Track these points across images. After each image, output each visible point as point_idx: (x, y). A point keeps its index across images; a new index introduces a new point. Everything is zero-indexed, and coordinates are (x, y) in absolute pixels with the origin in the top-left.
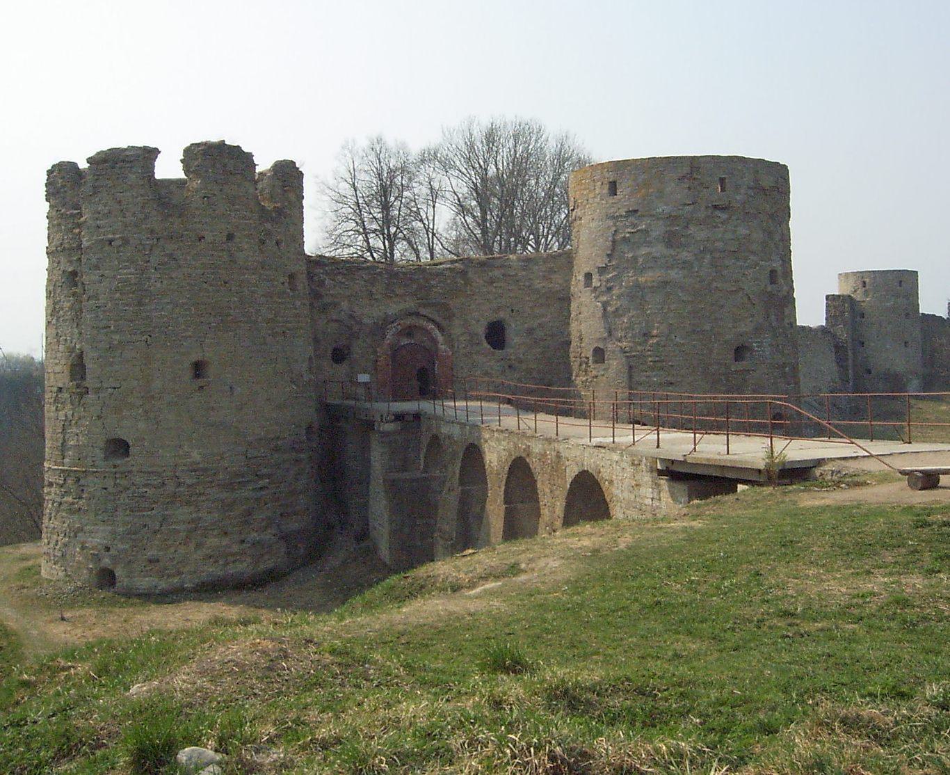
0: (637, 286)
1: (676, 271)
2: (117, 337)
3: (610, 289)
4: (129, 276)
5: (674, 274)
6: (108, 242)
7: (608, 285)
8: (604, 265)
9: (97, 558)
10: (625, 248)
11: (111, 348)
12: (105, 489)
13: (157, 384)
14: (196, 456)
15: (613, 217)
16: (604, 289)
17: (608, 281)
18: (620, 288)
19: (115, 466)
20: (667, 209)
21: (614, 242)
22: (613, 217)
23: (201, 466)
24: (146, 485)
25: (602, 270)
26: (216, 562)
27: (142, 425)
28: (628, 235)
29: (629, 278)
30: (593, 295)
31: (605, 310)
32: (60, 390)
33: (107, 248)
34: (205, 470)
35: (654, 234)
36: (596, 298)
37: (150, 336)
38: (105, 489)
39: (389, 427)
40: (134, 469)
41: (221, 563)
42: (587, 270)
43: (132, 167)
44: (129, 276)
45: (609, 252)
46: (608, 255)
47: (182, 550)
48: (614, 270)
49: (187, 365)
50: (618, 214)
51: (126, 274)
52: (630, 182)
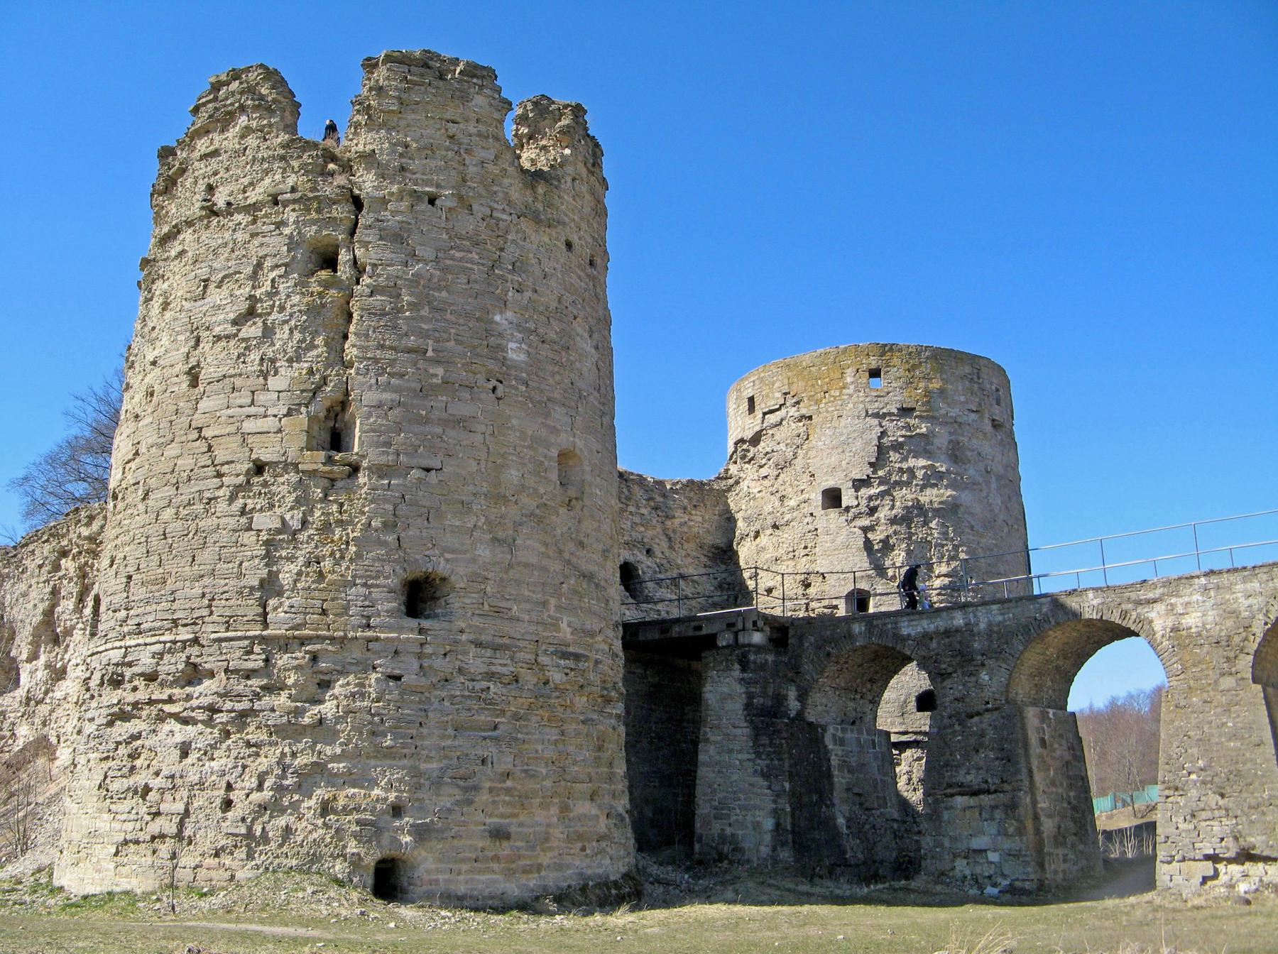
0: (918, 506)
1: (966, 492)
2: (440, 371)
3: (873, 511)
4: (469, 265)
5: (966, 498)
6: (426, 199)
7: (872, 504)
8: (865, 477)
9: (371, 830)
10: (894, 456)
11: (424, 391)
12: (397, 678)
13: (513, 475)
14: (565, 632)
15: (876, 415)
16: (863, 509)
17: (870, 498)
18: (893, 507)
19: (421, 631)
20: (953, 412)
21: (880, 447)
22: (876, 415)
23: (571, 649)
24: (490, 676)
25: (859, 484)
26: (583, 849)
27: (484, 552)
28: (901, 439)
29: (904, 496)
30: (844, 518)
31: (866, 537)
32: (259, 468)
33: (424, 206)
34: (577, 657)
35: (936, 441)
36: (849, 522)
37: (501, 382)
38: (397, 678)
39: (757, 638)
40: (464, 637)
41: (588, 851)
42: (830, 483)
43: (481, 87)
44: (469, 265)
45: (873, 460)
46: (871, 464)
47: (540, 816)
48: (880, 484)
49: (554, 452)
50: (885, 411)
51: (461, 260)
52: (902, 372)
